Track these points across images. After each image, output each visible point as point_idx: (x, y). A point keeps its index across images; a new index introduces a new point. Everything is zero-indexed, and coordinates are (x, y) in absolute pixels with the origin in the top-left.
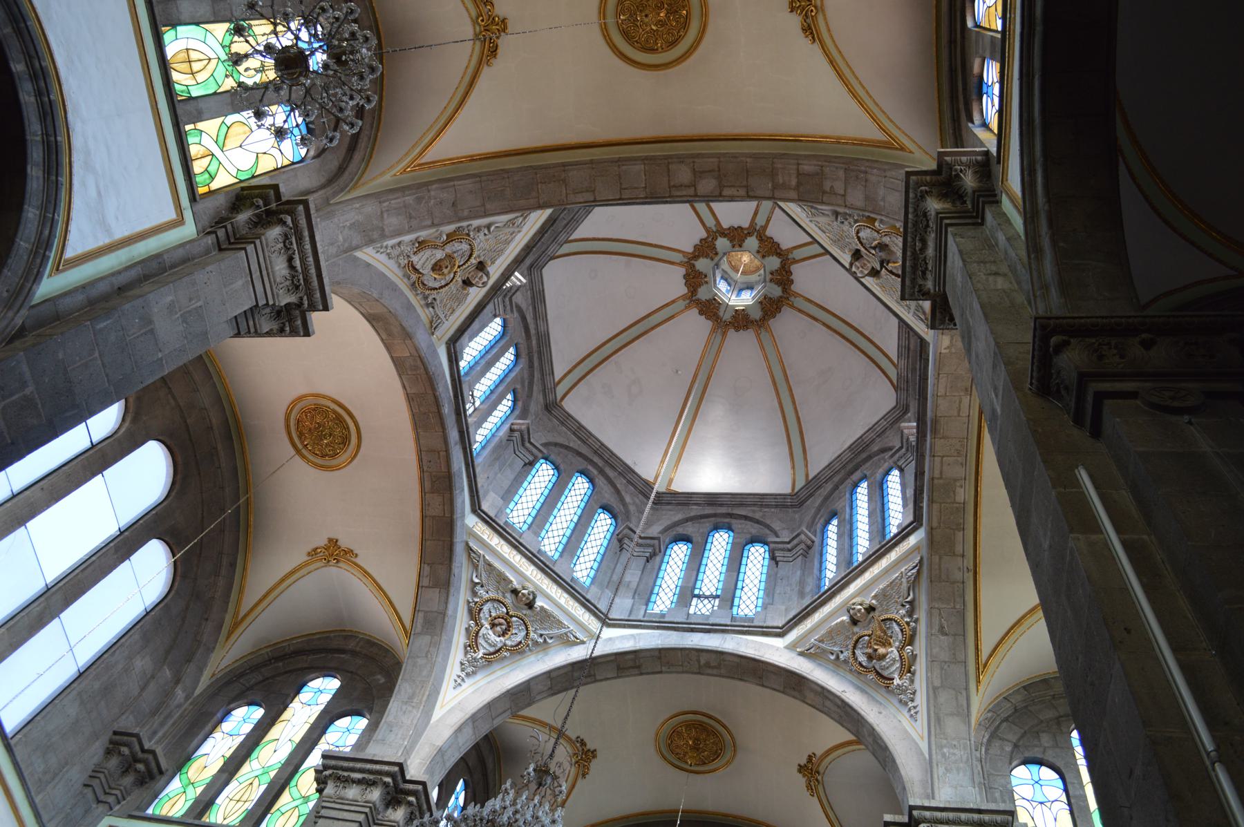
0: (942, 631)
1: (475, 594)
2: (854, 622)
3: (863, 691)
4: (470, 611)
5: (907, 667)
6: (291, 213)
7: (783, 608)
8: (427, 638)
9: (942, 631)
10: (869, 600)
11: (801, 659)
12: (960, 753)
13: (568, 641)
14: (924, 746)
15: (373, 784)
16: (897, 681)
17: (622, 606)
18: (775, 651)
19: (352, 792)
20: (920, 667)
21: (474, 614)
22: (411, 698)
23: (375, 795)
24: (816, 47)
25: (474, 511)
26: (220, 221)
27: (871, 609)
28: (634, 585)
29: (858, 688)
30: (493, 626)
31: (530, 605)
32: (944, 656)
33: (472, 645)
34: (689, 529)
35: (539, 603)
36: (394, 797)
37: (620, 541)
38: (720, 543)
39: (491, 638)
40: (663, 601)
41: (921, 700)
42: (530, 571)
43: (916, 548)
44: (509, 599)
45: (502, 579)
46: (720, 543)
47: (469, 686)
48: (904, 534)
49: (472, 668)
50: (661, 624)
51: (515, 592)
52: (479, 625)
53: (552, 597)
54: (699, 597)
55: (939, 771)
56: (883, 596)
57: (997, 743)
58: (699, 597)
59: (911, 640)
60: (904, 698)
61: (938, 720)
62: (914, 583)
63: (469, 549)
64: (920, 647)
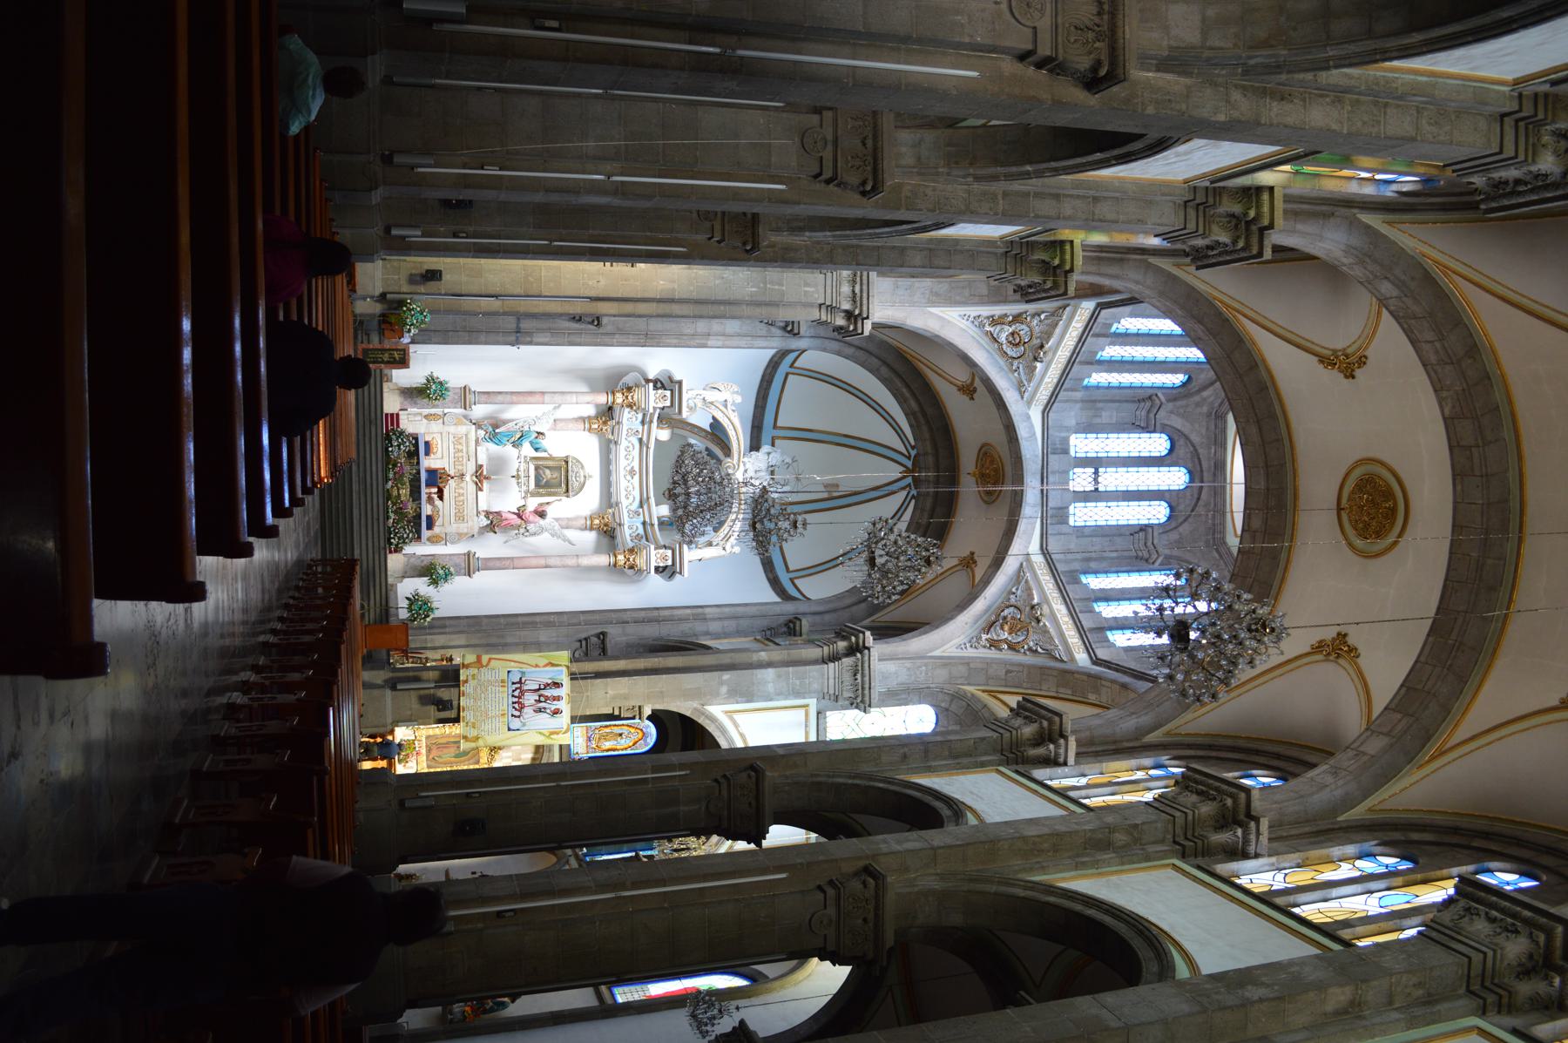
0: (1008, 672)
1: (1033, 316)
2: (1033, 607)
3: (986, 611)
4: (1020, 315)
5: (994, 644)
6: (1055, 286)
7: (1072, 546)
8: (985, 292)
9: (1008, 672)
10: (1045, 621)
11: (1017, 565)
12: (922, 677)
13: (1020, 388)
14: (937, 653)
15: (854, 301)
16: (984, 637)
17: (1068, 414)
18: (1027, 542)
19: (846, 289)
20: (993, 654)
21: (1017, 318)
22: (937, 294)
23: (846, 306)
24: (1308, 649)
25: (1098, 305)
26: (1032, 246)
27: (1038, 621)
28: (1098, 420)
29: (989, 608)
30: (1012, 334)
31: (1036, 359)
32: (991, 671)
33: (994, 321)
34: (1181, 451)
35: (1038, 365)
36: (849, 315)
37: (1150, 397)
38: (1176, 478)
39: (1004, 334)
40: (1082, 445)
41: (971, 652)
42: (1063, 354)
43: (1073, 659)
44: (1036, 342)
45: (1049, 335)
46: (1176, 478)
47: (964, 324)
48: (1089, 649)
49: (978, 322)
50: (1055, 447)
51: (1042, 347)
52: (1010, 324)
53: (1049, 373)
54: (1096, 473)
55: (908, 664)
56: (1045, 631)
57: (947, 698)
58: (1096, 473)
59: (1012, 647)
60: (974, 642)
61: (945, 665)
62: (1049, 654)
63: (1064, 308)
64: (1007, 655)
